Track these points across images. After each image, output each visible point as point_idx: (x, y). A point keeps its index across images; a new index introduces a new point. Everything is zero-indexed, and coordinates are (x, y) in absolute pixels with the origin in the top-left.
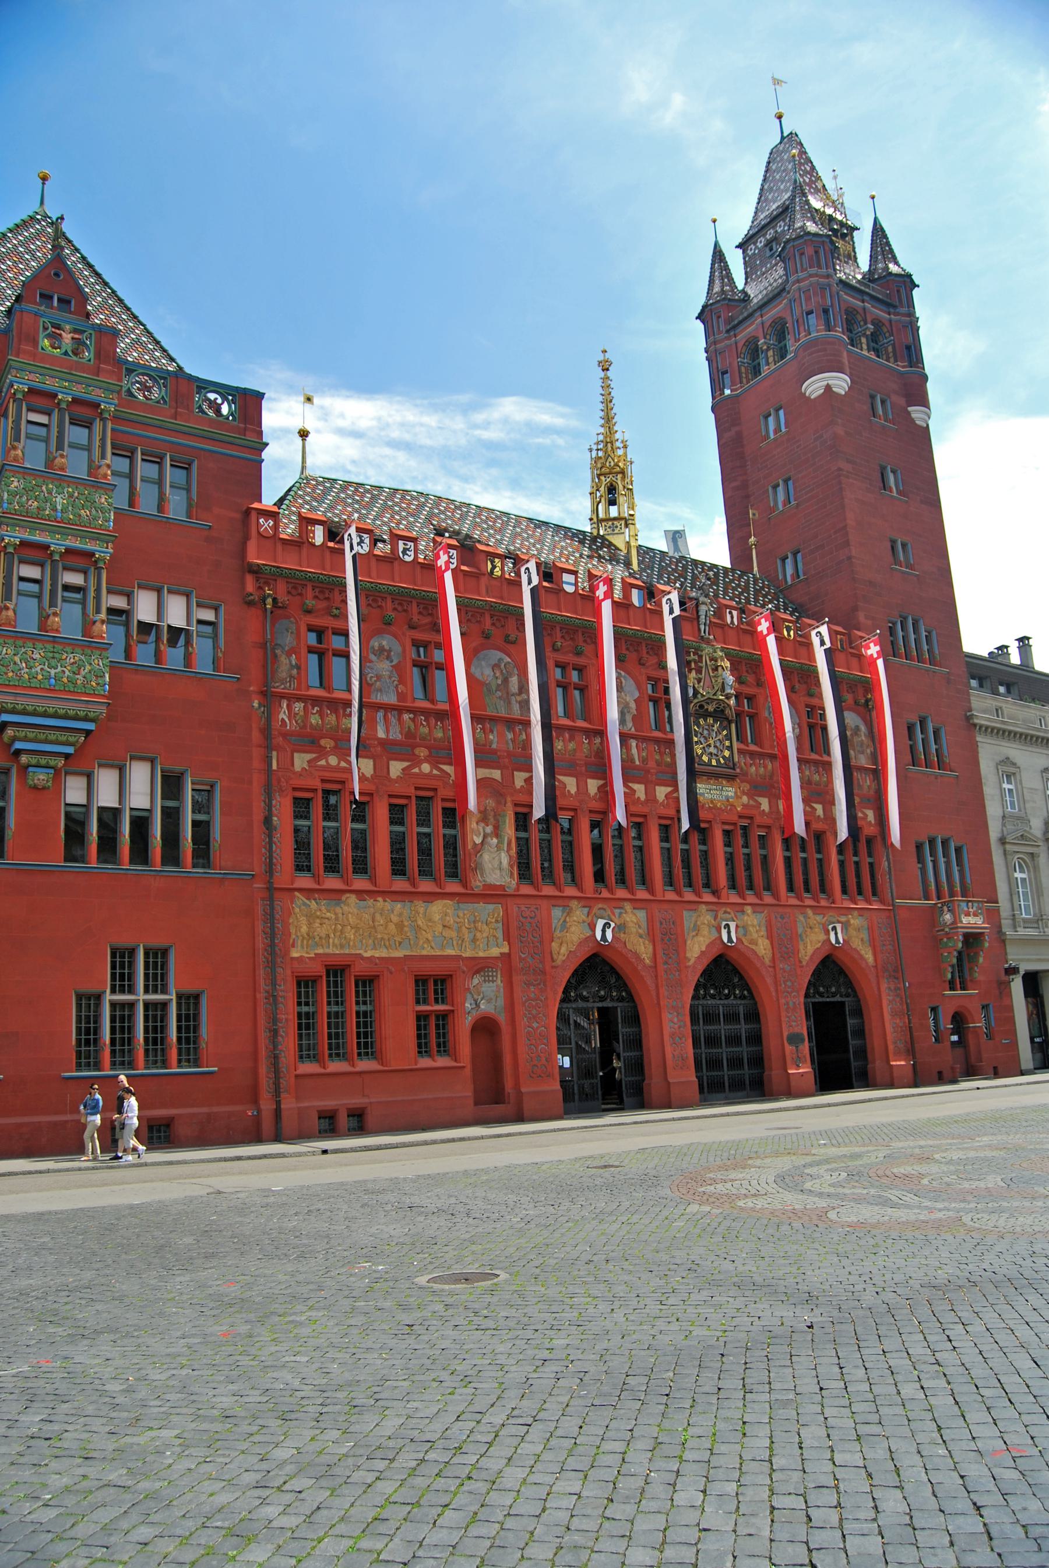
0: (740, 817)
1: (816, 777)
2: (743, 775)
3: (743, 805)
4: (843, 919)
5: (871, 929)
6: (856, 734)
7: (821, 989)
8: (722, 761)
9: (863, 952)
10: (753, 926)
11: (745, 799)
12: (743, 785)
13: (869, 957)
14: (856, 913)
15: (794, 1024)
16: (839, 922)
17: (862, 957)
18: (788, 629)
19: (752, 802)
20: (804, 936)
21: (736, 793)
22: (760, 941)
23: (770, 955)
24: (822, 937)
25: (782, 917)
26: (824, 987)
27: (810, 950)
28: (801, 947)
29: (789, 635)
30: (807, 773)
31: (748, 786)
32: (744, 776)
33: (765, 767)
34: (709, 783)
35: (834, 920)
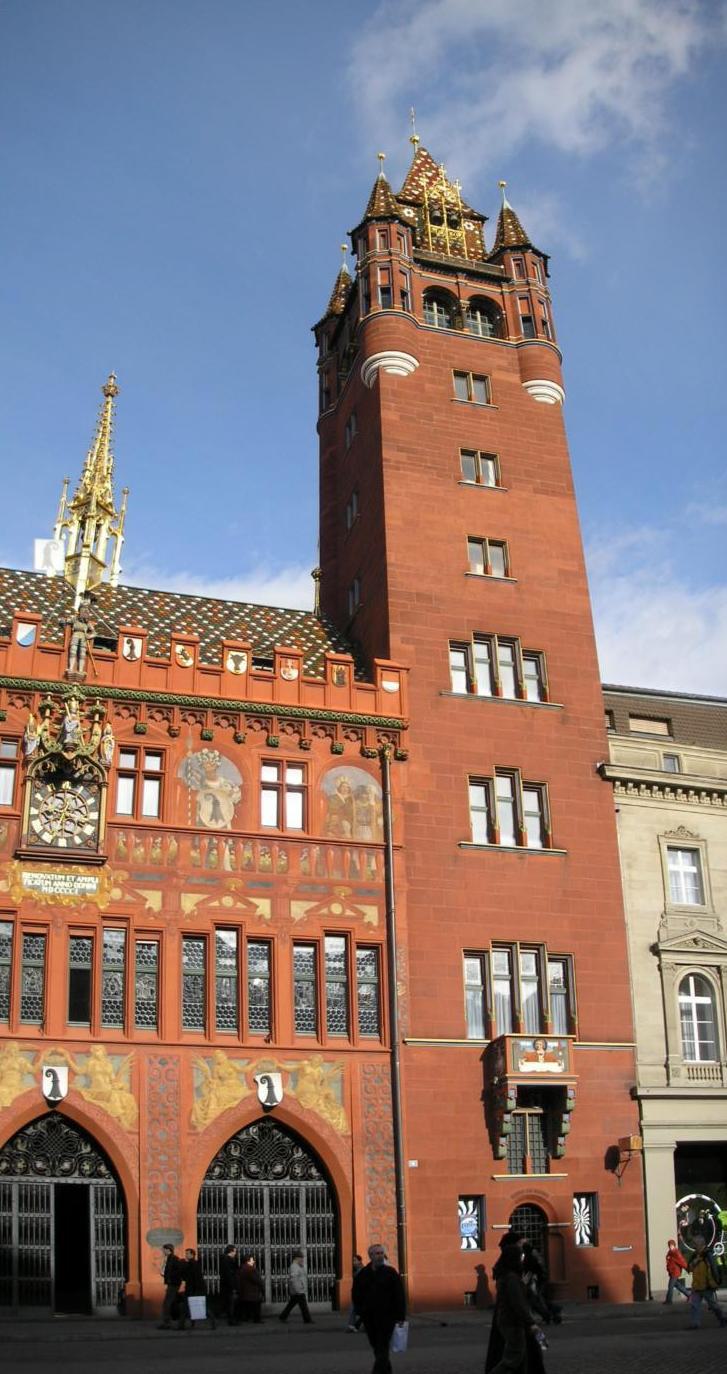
0: (104, 918)
1: (266, 860)
2: (118, 859)
3: (112, 902)
4: (290, 1066)
5: (346, 1082)
6: (358, 797)
7: (253, 1168)
8: (78, 840)
9: (326, 1115)
10: (105, 1073)
11: (116, 893)
12: (117, 872)
13: (339, 1122)
14: (318, 1057)
15: (163, 1215)
16: (279, 1070)
17: (323, 1123)
18: (237, 660)
19: (128, 897)
20: (205, 1091)
21: (100, 886)
22: (116, 1096)
23: (132, 1114)
24: (243, 1091)
25: (163, 1062)
26: (259, 1165)
27: (214, 1110)
28: (197, 1105)
29: (237, 668)
30: (248, 854)
31: (126, 875)
32: (122, 860)
33: (164, 847)
34: (55, 873)
35: (271, 1067)
